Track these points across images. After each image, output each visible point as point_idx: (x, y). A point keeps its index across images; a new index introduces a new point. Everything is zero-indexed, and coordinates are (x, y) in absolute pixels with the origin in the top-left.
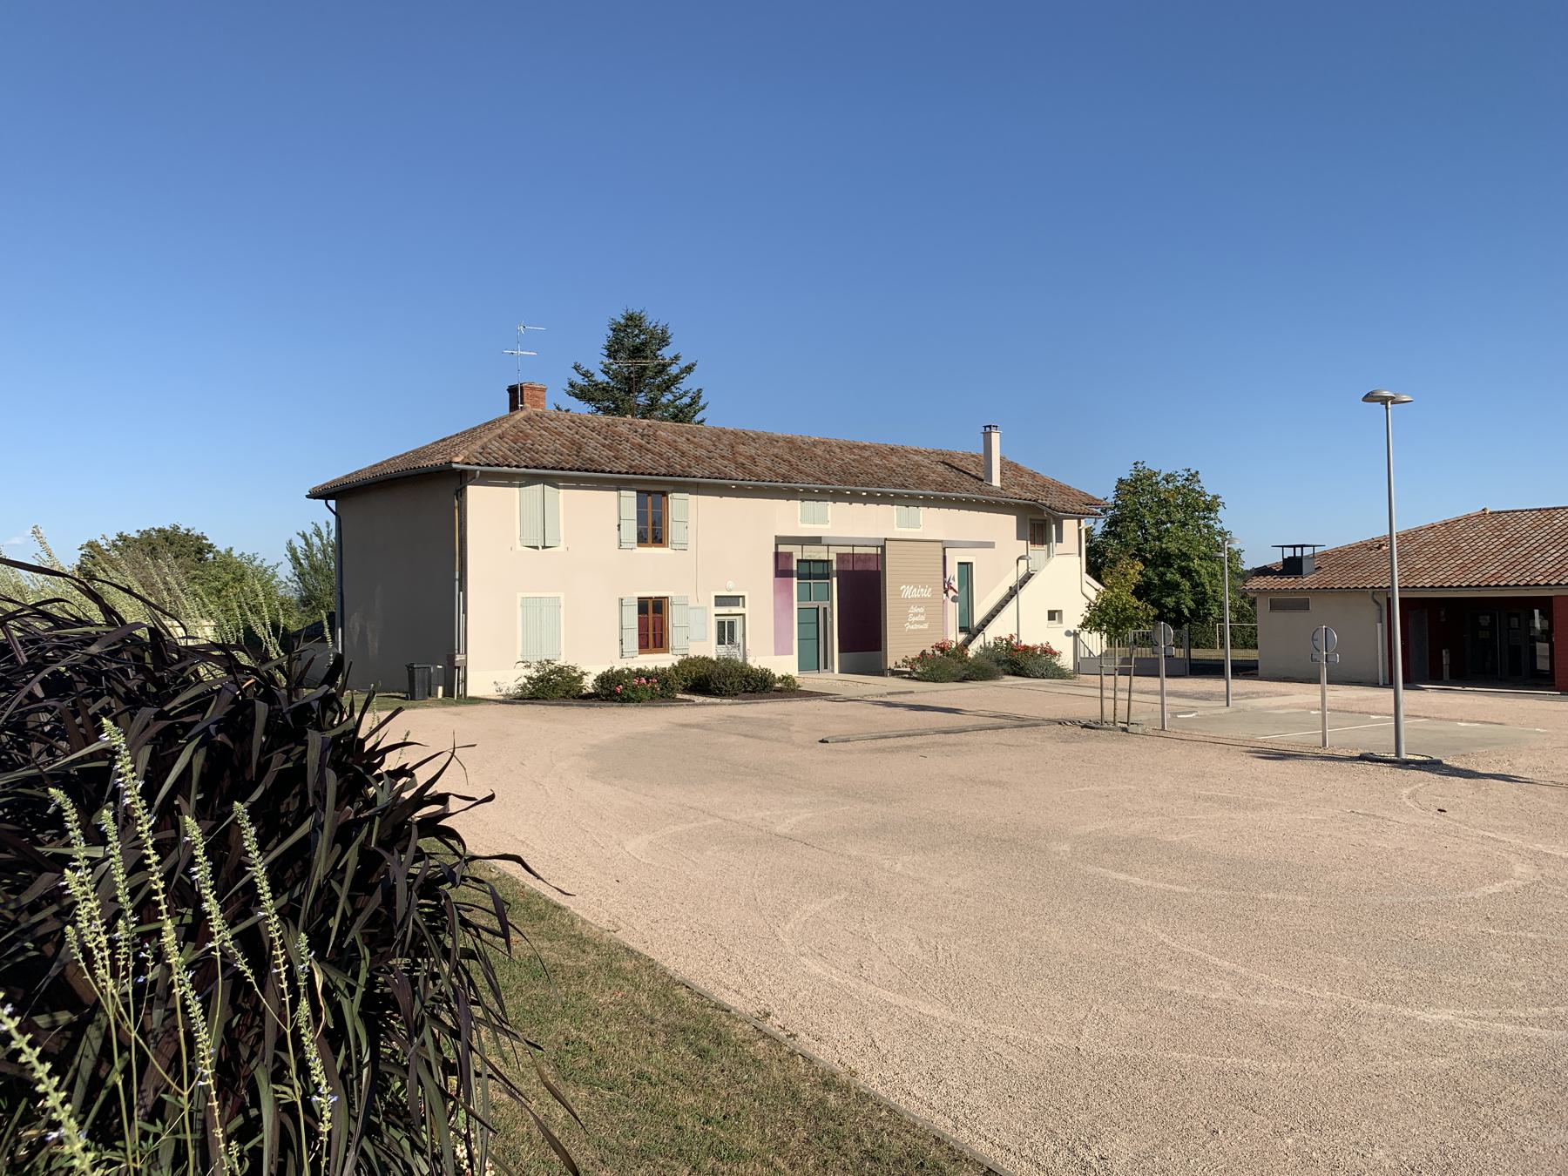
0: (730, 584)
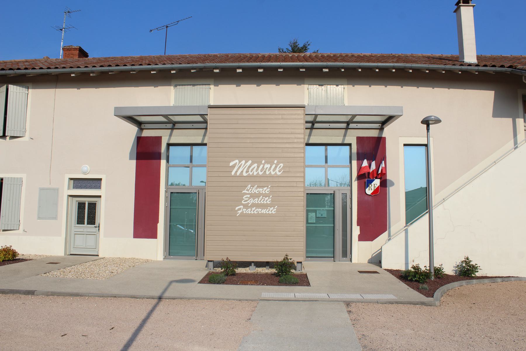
0: (86, 167)
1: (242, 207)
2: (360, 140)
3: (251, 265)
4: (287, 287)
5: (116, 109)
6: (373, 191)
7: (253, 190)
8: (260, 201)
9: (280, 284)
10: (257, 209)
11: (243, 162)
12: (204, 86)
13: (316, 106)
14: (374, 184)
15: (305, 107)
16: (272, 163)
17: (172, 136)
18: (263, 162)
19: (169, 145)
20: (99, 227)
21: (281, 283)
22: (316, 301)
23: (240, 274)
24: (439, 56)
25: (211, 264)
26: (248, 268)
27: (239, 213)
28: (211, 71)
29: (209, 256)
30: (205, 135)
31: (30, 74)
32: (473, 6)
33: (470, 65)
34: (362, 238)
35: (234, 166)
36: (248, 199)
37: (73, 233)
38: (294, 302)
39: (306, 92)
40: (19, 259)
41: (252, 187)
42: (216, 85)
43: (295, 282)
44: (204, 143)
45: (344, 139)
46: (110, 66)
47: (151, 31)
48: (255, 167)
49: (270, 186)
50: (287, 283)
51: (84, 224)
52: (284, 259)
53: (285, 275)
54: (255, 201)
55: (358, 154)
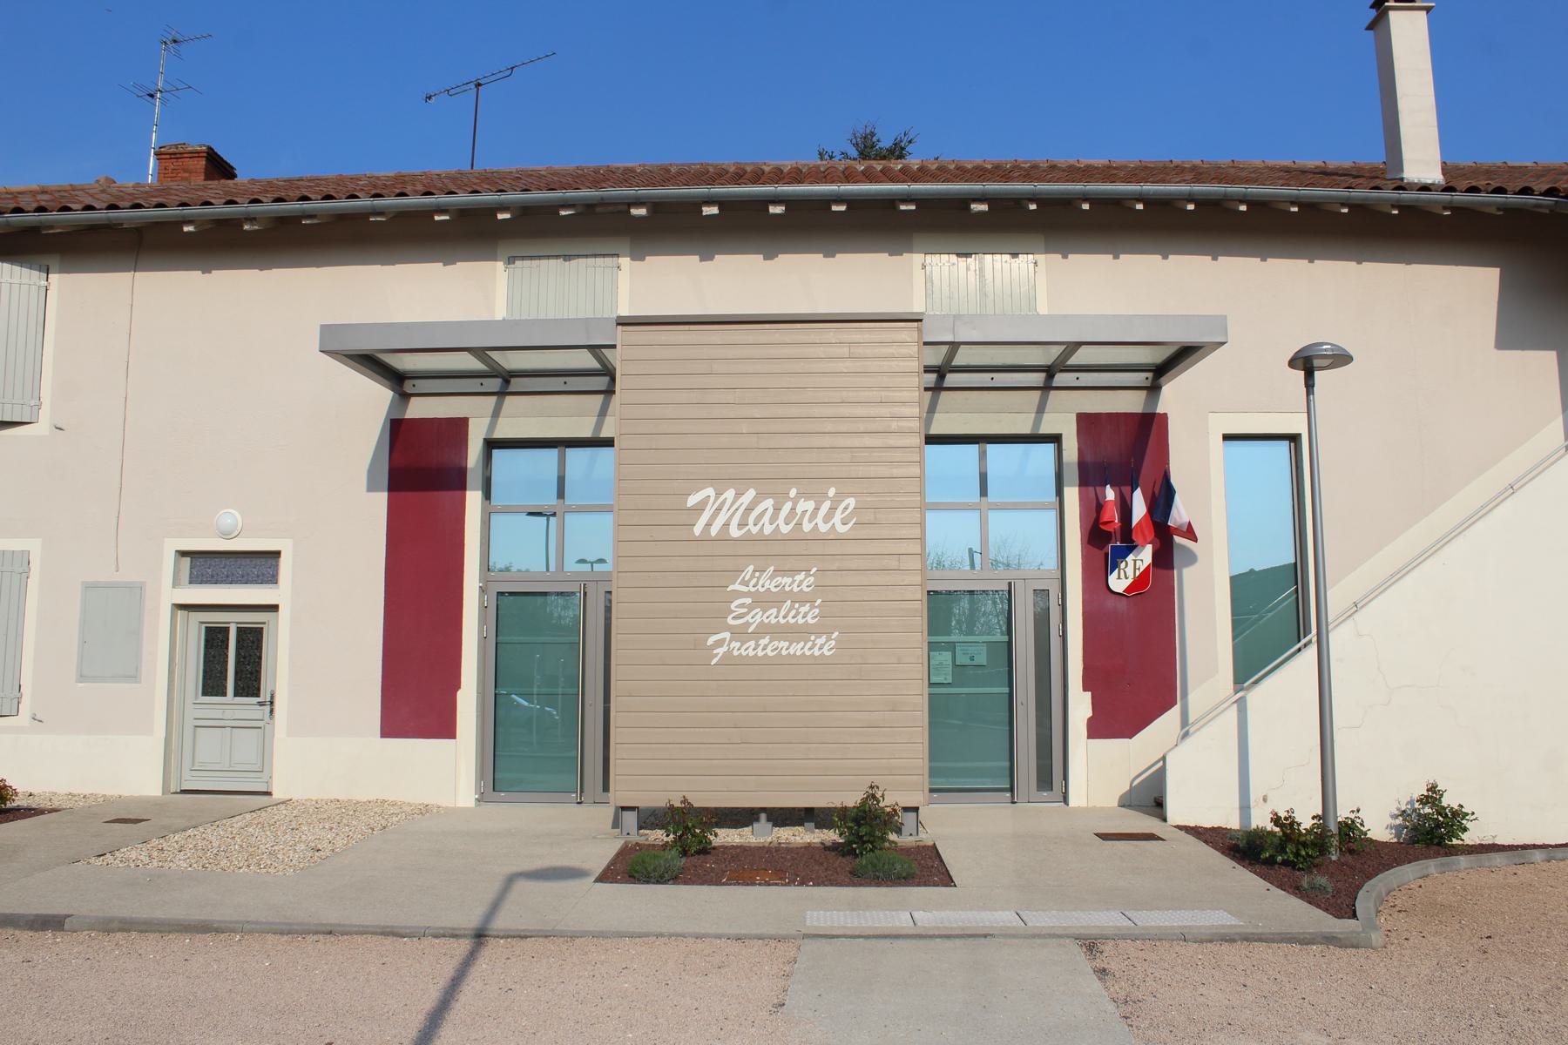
0: (230, 517)
1: (727, 635)
2: (1087, 423)
3: (757, 820)
4: (883, 890)
5: (326, 330)
6: (1130, 581)
7: (761, 583)
8: (784, 617)
9: (856, 880)
10: (776, 643)
11: (730, 494)
12: (599, 261)
13: (957, 317)
14: (1135, 561)
15: (921, 320)
16: (819, 498)
17: (501, 415)
18: (793, 493)
19: (491, 445)
20: (272, 703)
21: (858, 878)
22: (985, 936)
23: (725, 848)
24: (1317, 167)
25: (630, 819)
26: (747, 830)
27: (720, 655)
28: (619, 212)
29: (622, 793)
30: (603, 413)
31: (52, 227)
32: (1428, 10)
33: (1425, 188)
34: (1099, 728)
35: (699, 508)
36: (746, 610)
37: (189, 723)
38: (914, 941)
39: (919, 277)
40: (18, 809)
41: (757, 574)
42: (637, 256)
43: (904, 874)
44: (601, 436)
45: (1037, 422)
46: (305, 198)
47: (430, 98)
48: (767, 509)
49: (814, 570)
50: (878, 878)
51: (224, 694)
52: (864, 801)
53: (871, 850)
54: (767, 618)
55: (1082, 466)
